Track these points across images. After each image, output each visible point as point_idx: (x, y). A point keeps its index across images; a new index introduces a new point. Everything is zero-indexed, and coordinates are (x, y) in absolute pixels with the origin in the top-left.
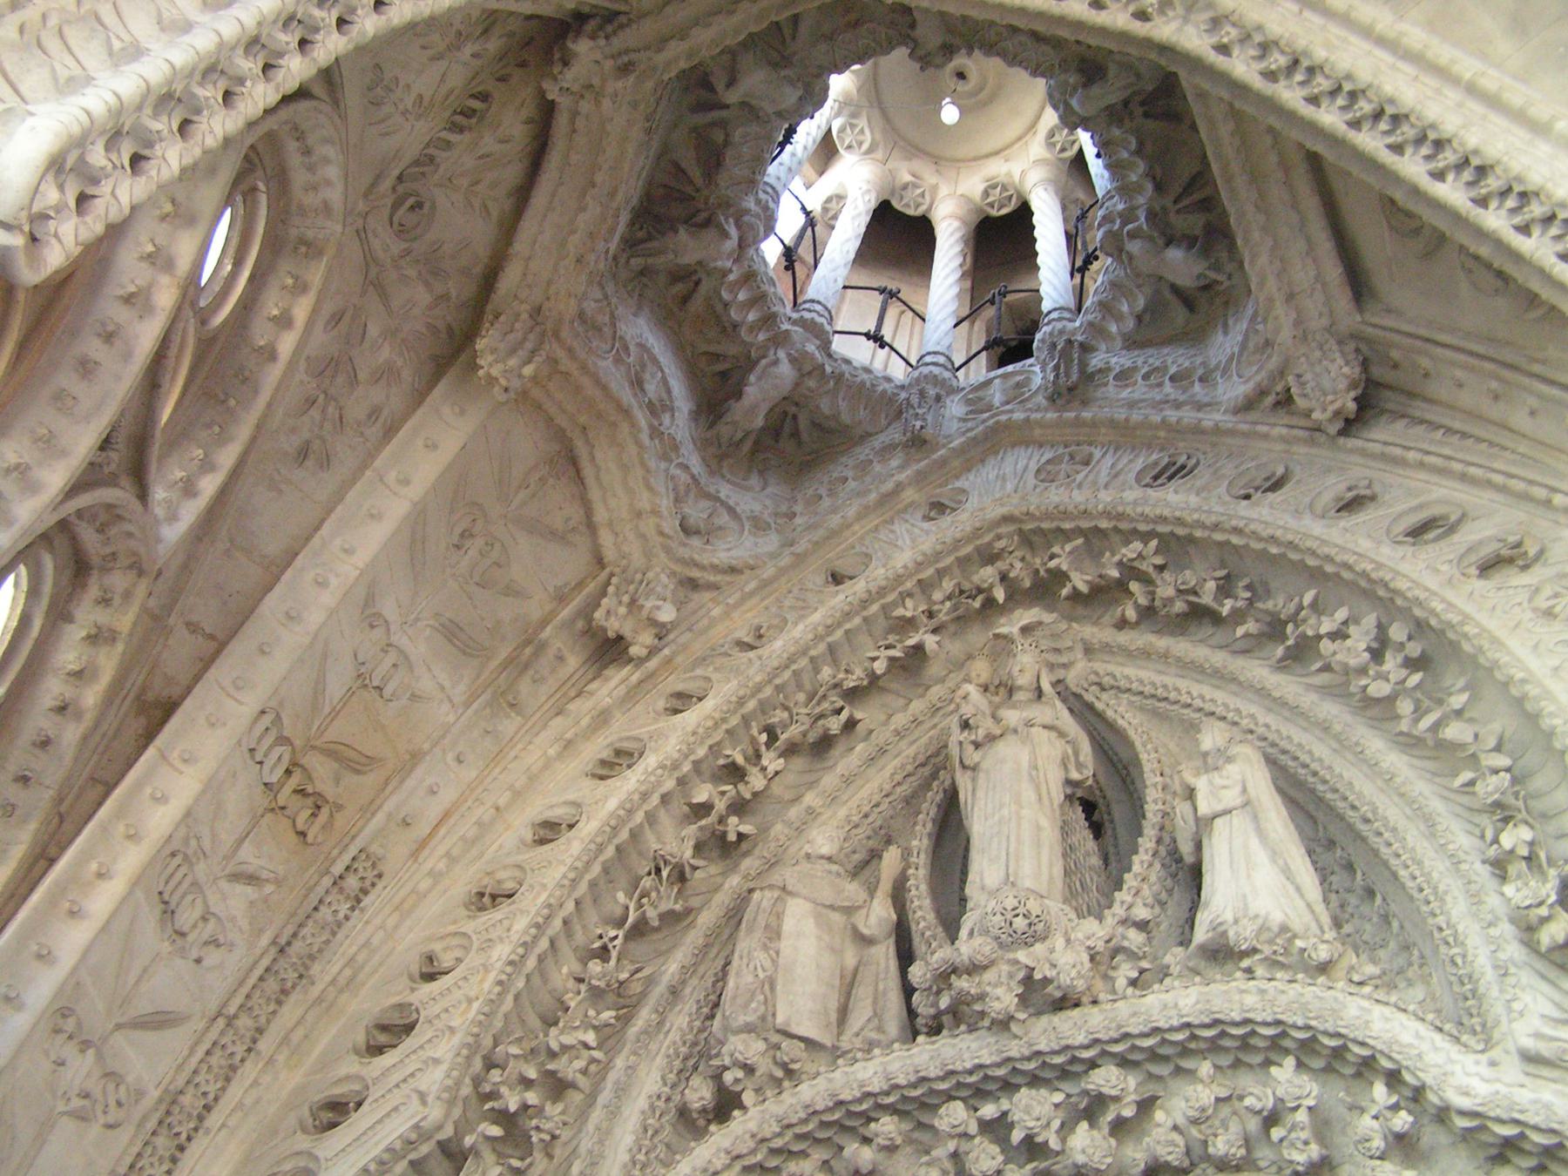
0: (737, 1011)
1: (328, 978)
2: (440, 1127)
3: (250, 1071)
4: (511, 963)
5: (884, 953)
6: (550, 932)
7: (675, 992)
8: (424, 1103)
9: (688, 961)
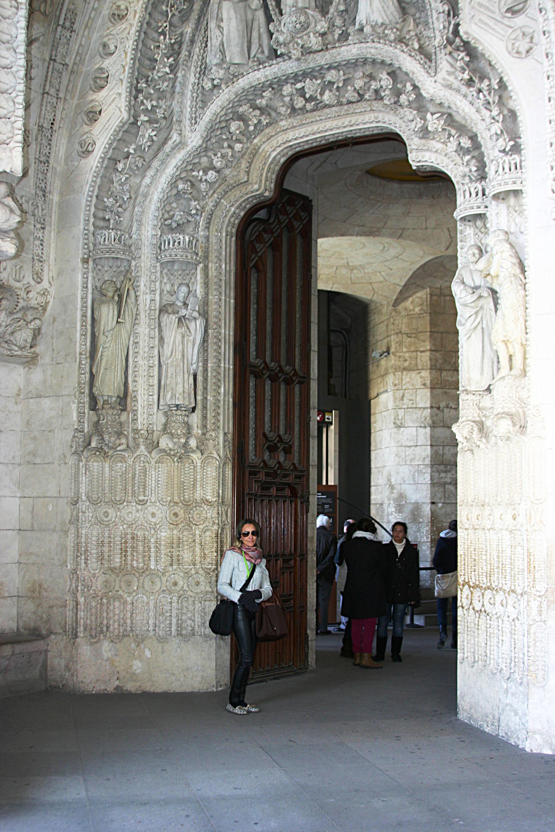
0: (213, 59)
1: (72, 61)
2: (129, 119)
3: (60, 106)
4: (133, 49)
5: (260, 15)
6: (143, 30)
7: (192, 41)
8: (121, 112)
9: (194, 26)
